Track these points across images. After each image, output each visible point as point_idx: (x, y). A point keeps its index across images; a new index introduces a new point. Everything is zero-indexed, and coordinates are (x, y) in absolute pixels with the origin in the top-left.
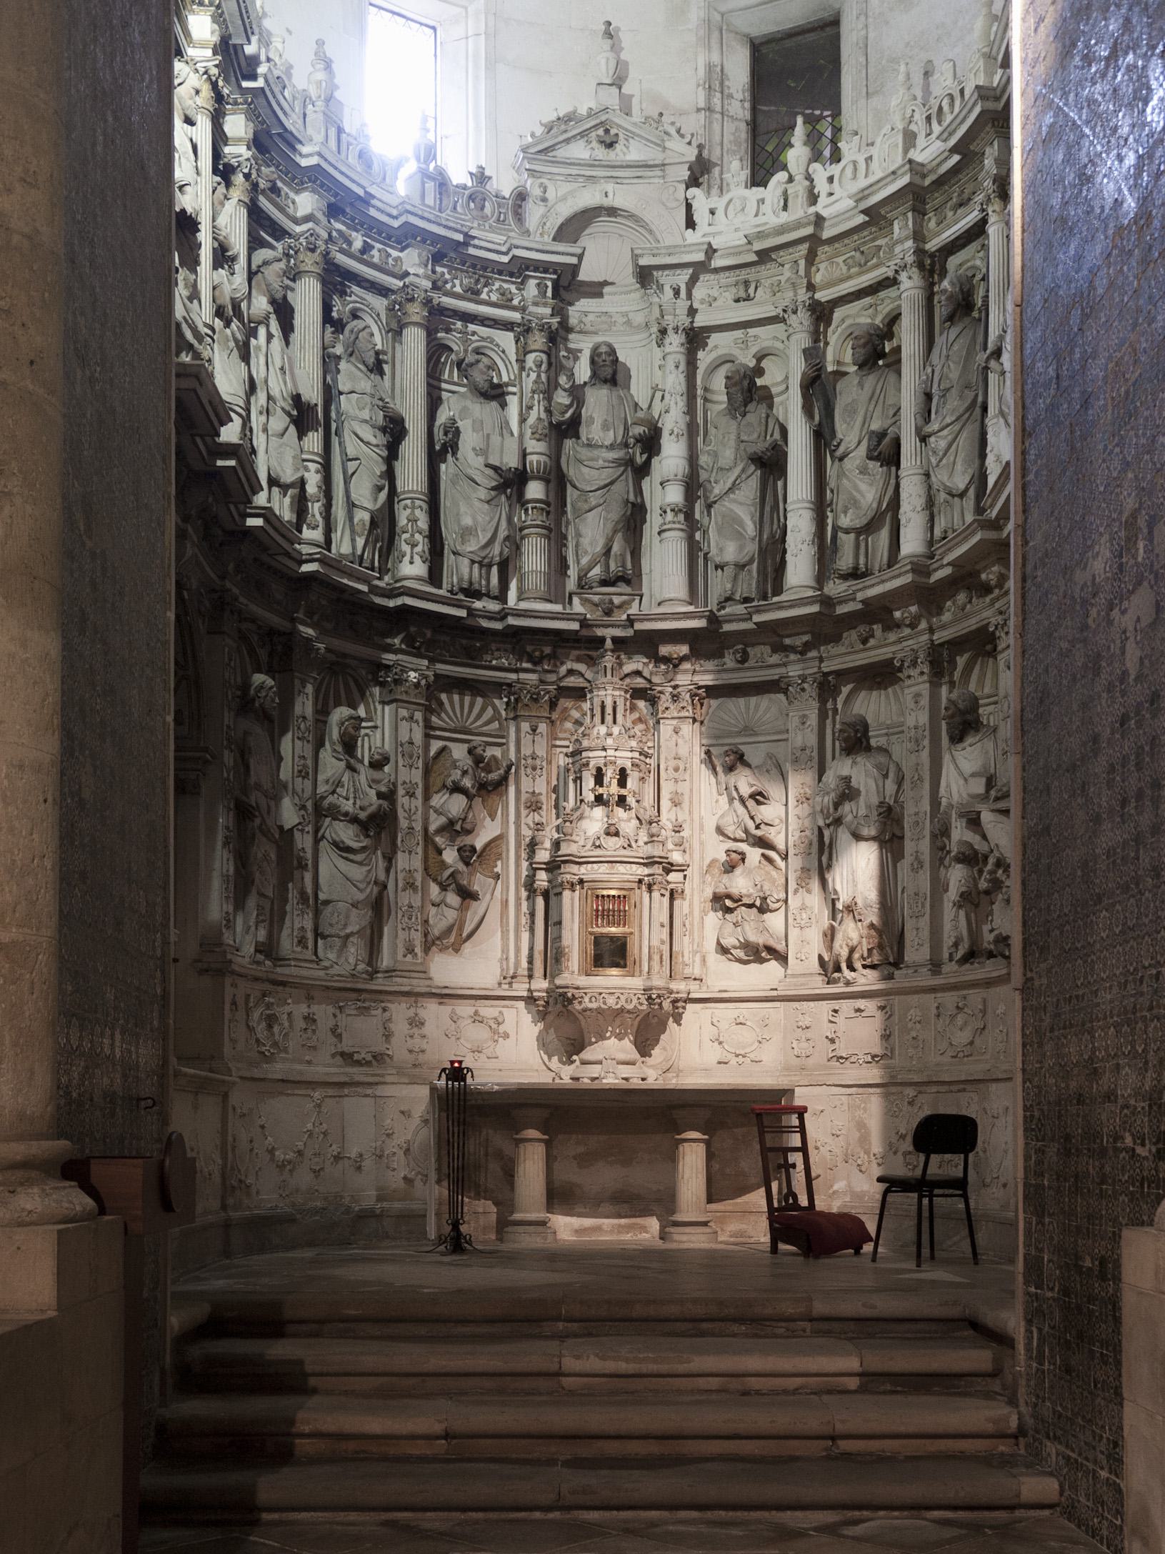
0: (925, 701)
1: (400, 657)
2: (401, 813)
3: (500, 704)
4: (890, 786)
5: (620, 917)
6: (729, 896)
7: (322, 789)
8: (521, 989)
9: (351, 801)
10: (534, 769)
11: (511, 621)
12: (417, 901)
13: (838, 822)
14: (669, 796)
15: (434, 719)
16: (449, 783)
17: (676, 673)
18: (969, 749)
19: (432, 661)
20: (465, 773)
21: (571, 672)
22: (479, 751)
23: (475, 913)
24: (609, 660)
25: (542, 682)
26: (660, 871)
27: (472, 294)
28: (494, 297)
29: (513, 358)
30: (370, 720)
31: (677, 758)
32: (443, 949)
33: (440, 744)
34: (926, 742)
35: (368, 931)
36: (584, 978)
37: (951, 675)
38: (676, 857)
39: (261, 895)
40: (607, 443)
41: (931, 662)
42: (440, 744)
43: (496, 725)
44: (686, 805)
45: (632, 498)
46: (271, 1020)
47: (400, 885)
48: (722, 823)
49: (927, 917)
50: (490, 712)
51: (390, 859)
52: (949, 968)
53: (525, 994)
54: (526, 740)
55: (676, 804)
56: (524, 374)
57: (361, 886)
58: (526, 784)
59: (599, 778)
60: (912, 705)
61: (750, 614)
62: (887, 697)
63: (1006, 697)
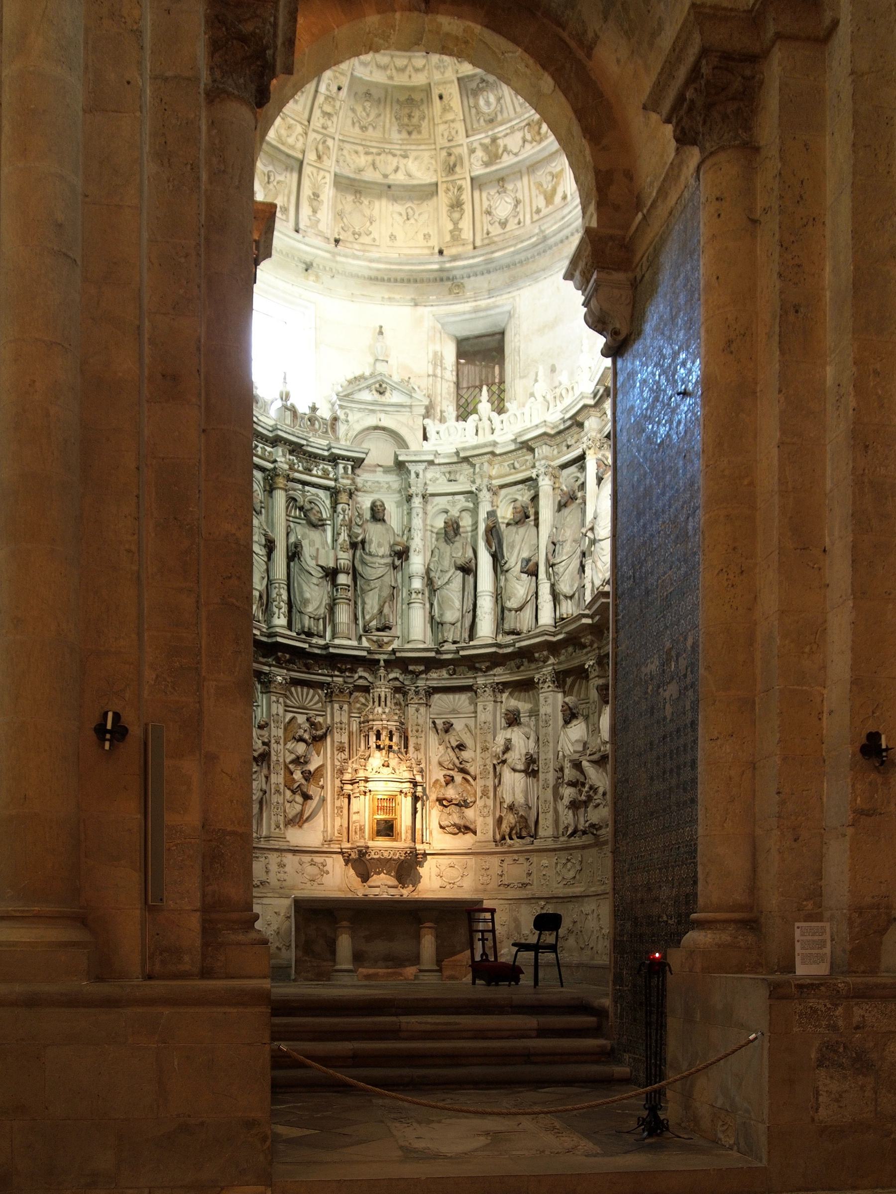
1: (272, 668)
2: (273, 753)
4: (532, 743)
5: (392, 810)
6: (445, 799)
10: (341, 729)
11: (331, 650)
12: (281, 801)
14: (413, 745)
15: (288, 701)
16: (297, 737)
17: (417, 680)
19: (288, 670)
20: (305, 731)
21: (360, 677)
22: (313, 719)
24: (382, 672)
25: (345, 682)
26: (412, 786)
28: (320, 473)
29: (329, 506)
33: (291, 715)
37: (564, 688)
38: (419, 778)
40: (380, 554)
44: (422, 750)
45: (393, 584)
48: (441, 760)
49: (551, 813)
50: (317, 698)
51: (267, 777)
53: (340, 850)
54: (337, 713)
55: (417, 749)
56: (335, 514)
58: (337, 737)
62: (529, 697)
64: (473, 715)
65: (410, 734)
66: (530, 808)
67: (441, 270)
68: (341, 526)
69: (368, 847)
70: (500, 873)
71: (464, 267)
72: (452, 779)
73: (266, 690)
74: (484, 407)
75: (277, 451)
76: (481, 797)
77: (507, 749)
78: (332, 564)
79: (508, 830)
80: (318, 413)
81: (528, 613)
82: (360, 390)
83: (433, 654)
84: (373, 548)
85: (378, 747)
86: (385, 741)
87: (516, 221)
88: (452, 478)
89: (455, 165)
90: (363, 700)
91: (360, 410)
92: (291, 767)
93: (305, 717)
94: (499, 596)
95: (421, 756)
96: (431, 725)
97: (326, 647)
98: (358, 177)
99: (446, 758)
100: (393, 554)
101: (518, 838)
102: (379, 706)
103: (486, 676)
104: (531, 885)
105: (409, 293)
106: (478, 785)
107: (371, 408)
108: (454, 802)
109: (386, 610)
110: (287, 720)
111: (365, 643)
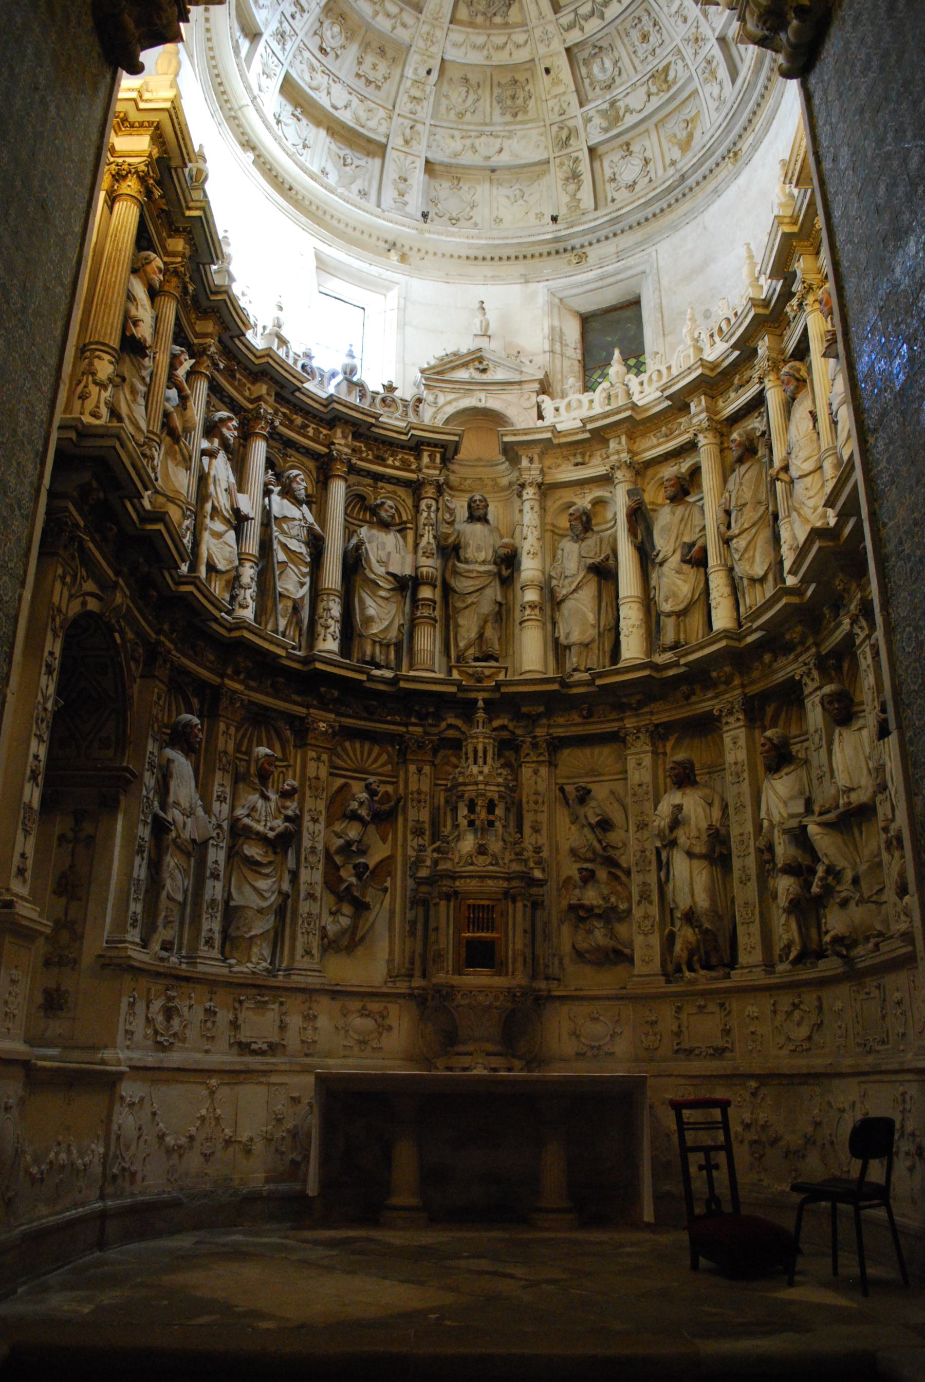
0: (742, 742)
1: (312, 711)
2: (305, 835)
4: (716, 813)
6: (582, 906)
8: (402, 987)
9: (263, 823)
10: (419, 802)
11: (402, 684)
13: (673, 843)
18: (785, 777)
20: (361, 804)
22: (374, 786)
23: (367, 920)
24: (481, 715)
27: (380, 460)
28: (397, 464)
29: (410, 506)
30: (284, 759)
31: (536, 793)
32: (338, 950)
33: (342, 781)
34: (746, 775)
35: (272, 934)
36: (456, 977)
38: (537, 874)
40: (481, 559)
41: (744, 710)
42: (342, 781)
43: (390, 767)
44: (544, 832)
45: (499, 599)
47: (302, 895)
50: (384, 757)
51: (295, 876)
52: (781, 967)
53: (407, 991)
55: (536, 830)
57: (266, 895)
58: (412, 814)
60: (731, 745)
61: (593, 680)
63: (816, 731)
65: (525, 806)
66: (720, 918)
67: (556, 240)
68: (425, 525)
69: (452, 987)
70: (676, 1029)
71: (585, 233)
72: (592, 873)
73: (302, 742)
74: (616, 368)
75: (335, 433)
76: (639, 903)
77: (676, 822)
78: (408, 571)
79: (685, 955)
80: (398, 394)
81: (696, 620)
82: (453, 368)
83: (555, 687)
84: (470, 553)
85: (471, 823)
87: (647, 179)
88: (579, 460)
89: (568, 138)
90: (454, 760)
91: (453, 390)
93: (363, 784)
94: (648, 602)
95: (543, 840)
96: (558, 793)
97: (394, 681)
98: (453, 161)
100: (498, 560)
101: (703, 968)
102: (475, 763)
103: (637, 715)
104: (732, 1051)
105: (519, 268)
107: (468, 386)
108: (597, 911)
109: (489, 633)
110: (335, 788)
111: (456, 675)
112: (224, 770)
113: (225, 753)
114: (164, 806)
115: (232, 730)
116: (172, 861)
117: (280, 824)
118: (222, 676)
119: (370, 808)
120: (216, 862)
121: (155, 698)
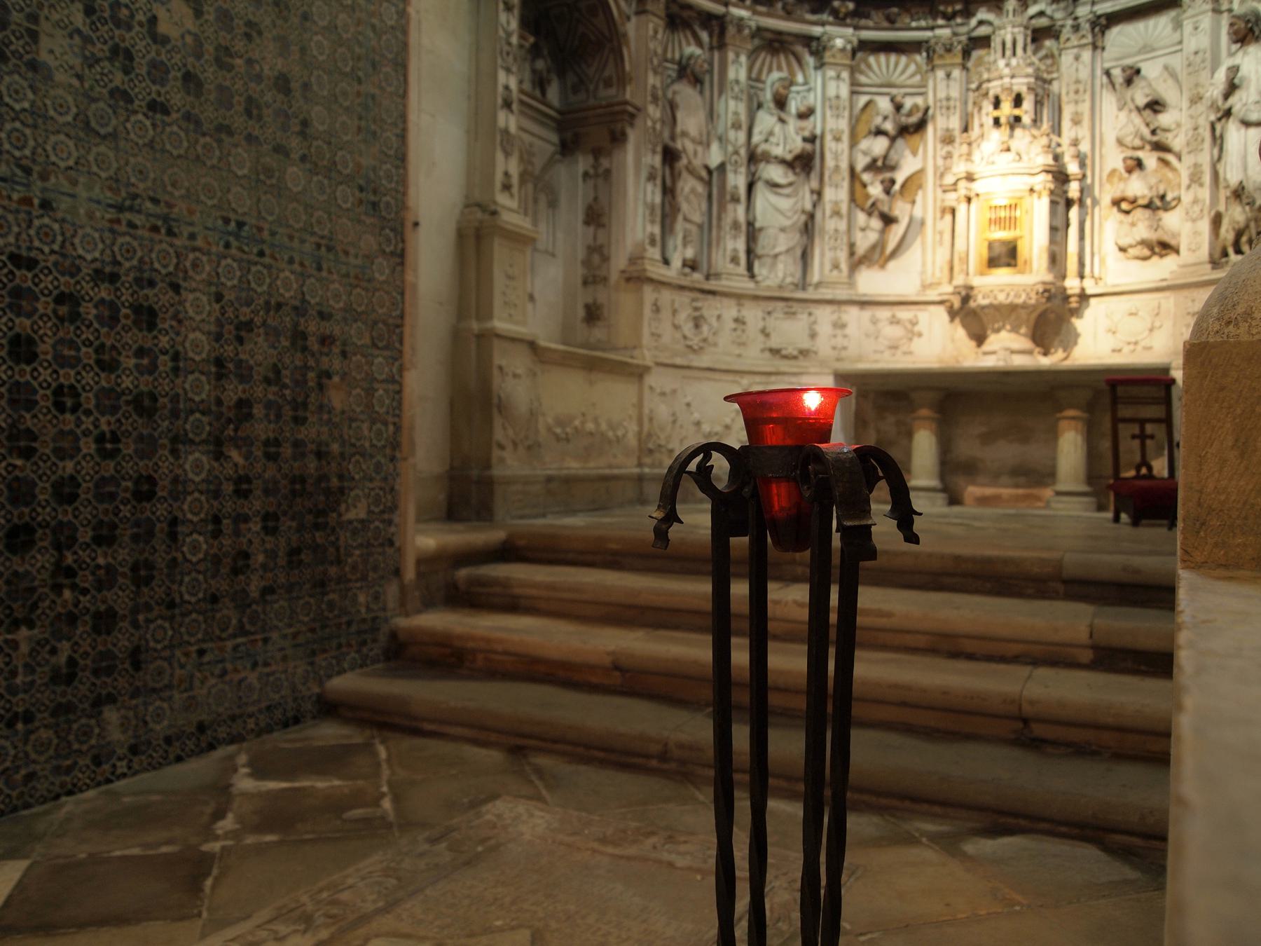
3: (920, 58)
5: (1011, 222)
6: (1123, 199)
7: (756, 138)
10: (948, 108)
13: (1228, 113)
15: (863, 79)
16: (873, 129)
17: (1075, 7)
19: (856, 28)
20: (885, 118)
21: (981, 23)
22: (899, 99)
25: (955, 34)
31: (1078, 81)
38: (1073, 168)
39: (686, 219)
43: (918, 78)
46: (697, 322)
47: (828, 213)
50: (912, 68)
51: (819, 193)
54: (942, 86)
55: (1076, 122)
57: (789, 214)
59: (997, 104)
64: (1178, 47)
65: (1064, 98)
69: (971, 288)
72: (1139, 164)
76: (1189, 187)
79: (1230, 237)
85: (997, 122)
86: (1007, 109)
92: (866, 177)
99: (1131, 129)
106: (1183, 169)
108: (1141, 202)
112: (736, 98)
113: (737, 82)
114: (673, 138)
115: (743, 59)
116: (688, 186)
117: (798, 145)
118: (726, 5)
119: (895, 121)
120: (736, 187)
121: (651, 32)
